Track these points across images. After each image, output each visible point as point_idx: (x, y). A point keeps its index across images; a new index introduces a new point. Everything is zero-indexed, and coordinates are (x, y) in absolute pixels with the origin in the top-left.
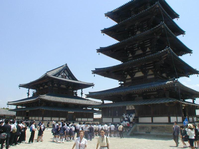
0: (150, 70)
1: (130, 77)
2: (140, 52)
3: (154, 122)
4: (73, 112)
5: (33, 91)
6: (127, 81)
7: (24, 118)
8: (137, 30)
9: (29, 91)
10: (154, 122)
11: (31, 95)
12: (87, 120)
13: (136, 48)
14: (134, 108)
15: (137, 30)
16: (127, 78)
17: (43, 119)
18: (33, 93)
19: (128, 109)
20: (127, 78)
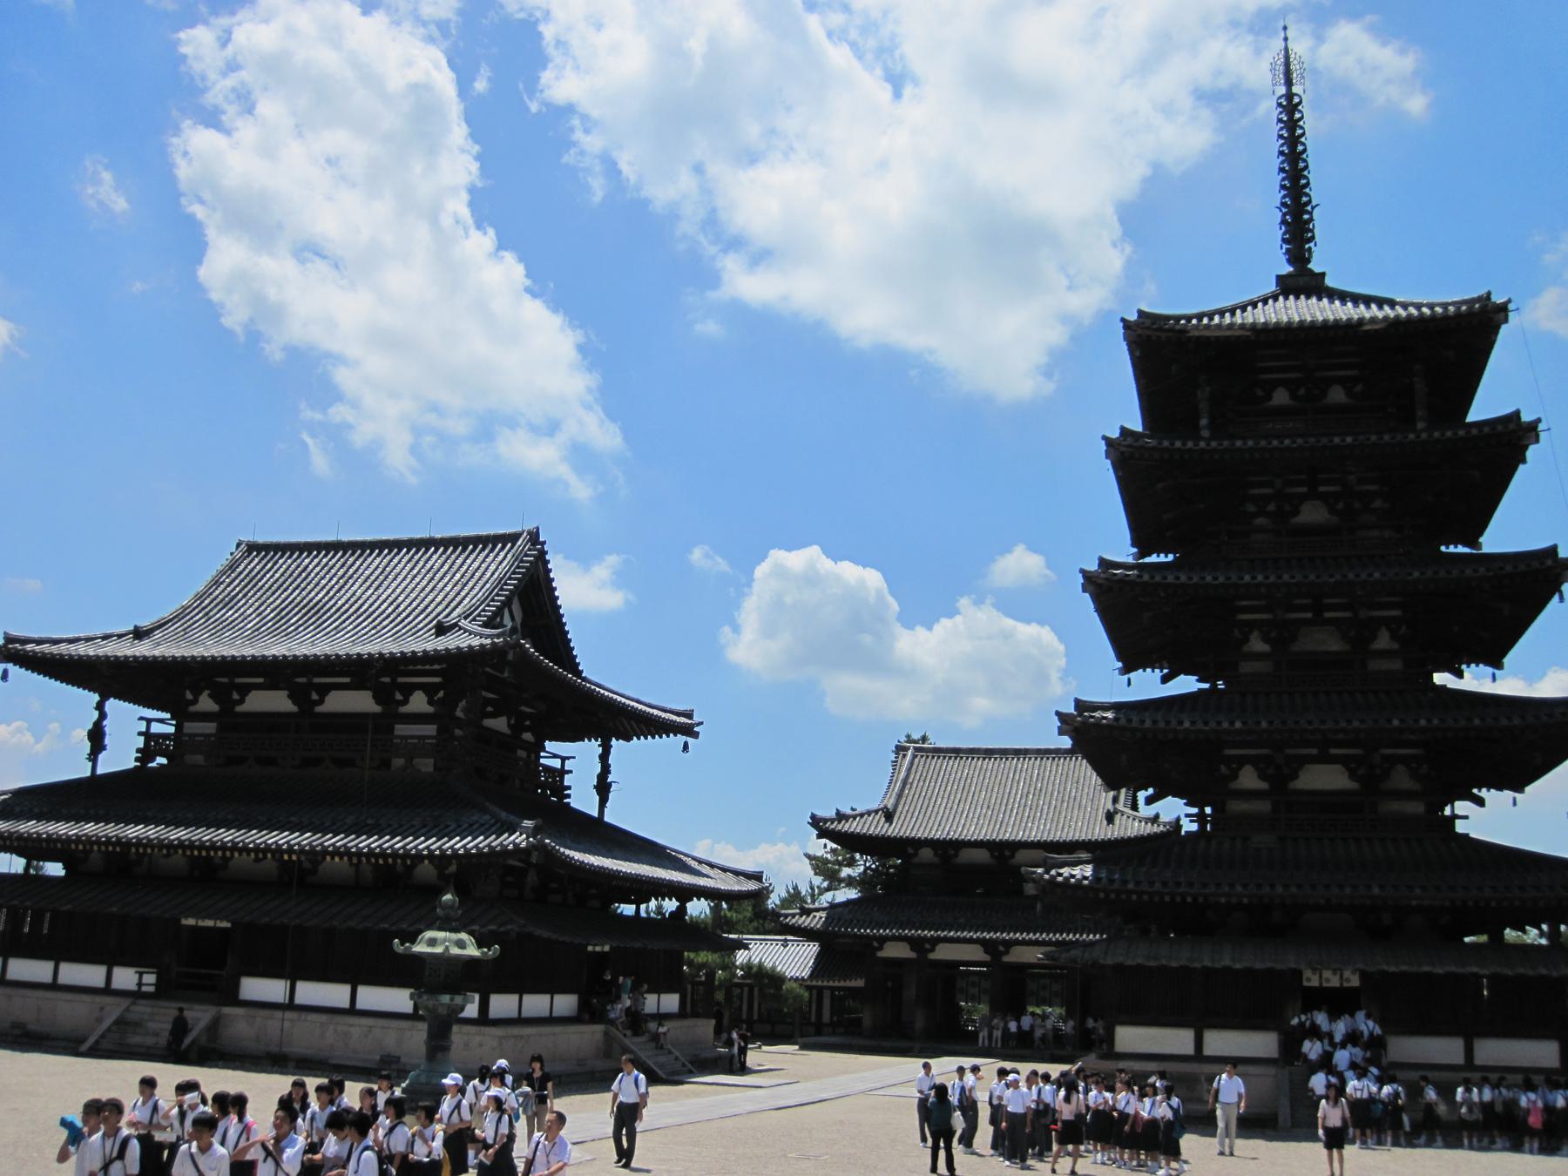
0: (1401, 768)
1: (1263, 785)
2: (1329, 642)
3: (1478, 1061)
4: (607, 948)
5: (149, 721)
6: (1236, 806)
7: (150, 978)
8: (1304, 490)
9: (103, 716)
10: (1478, 1061)
11: (120, 756)
12: (346, 1004)
13: (1303, 609)
14: (1355, 981)
15: (1304, 490)
16: (1234, 785)
17: (484, 1006)
18: (147, 735)
19: (1315, 983)
20: (1234, 785)
